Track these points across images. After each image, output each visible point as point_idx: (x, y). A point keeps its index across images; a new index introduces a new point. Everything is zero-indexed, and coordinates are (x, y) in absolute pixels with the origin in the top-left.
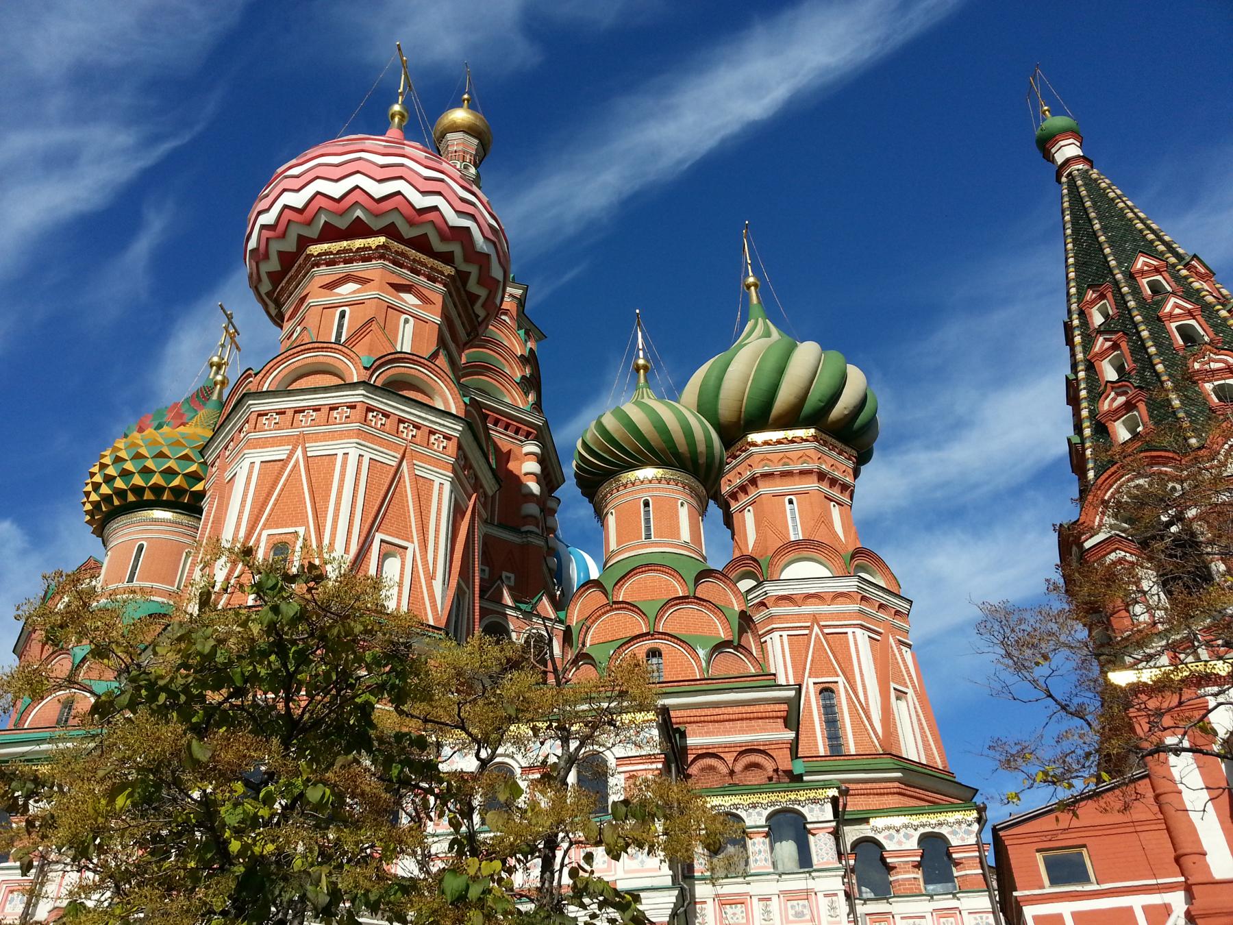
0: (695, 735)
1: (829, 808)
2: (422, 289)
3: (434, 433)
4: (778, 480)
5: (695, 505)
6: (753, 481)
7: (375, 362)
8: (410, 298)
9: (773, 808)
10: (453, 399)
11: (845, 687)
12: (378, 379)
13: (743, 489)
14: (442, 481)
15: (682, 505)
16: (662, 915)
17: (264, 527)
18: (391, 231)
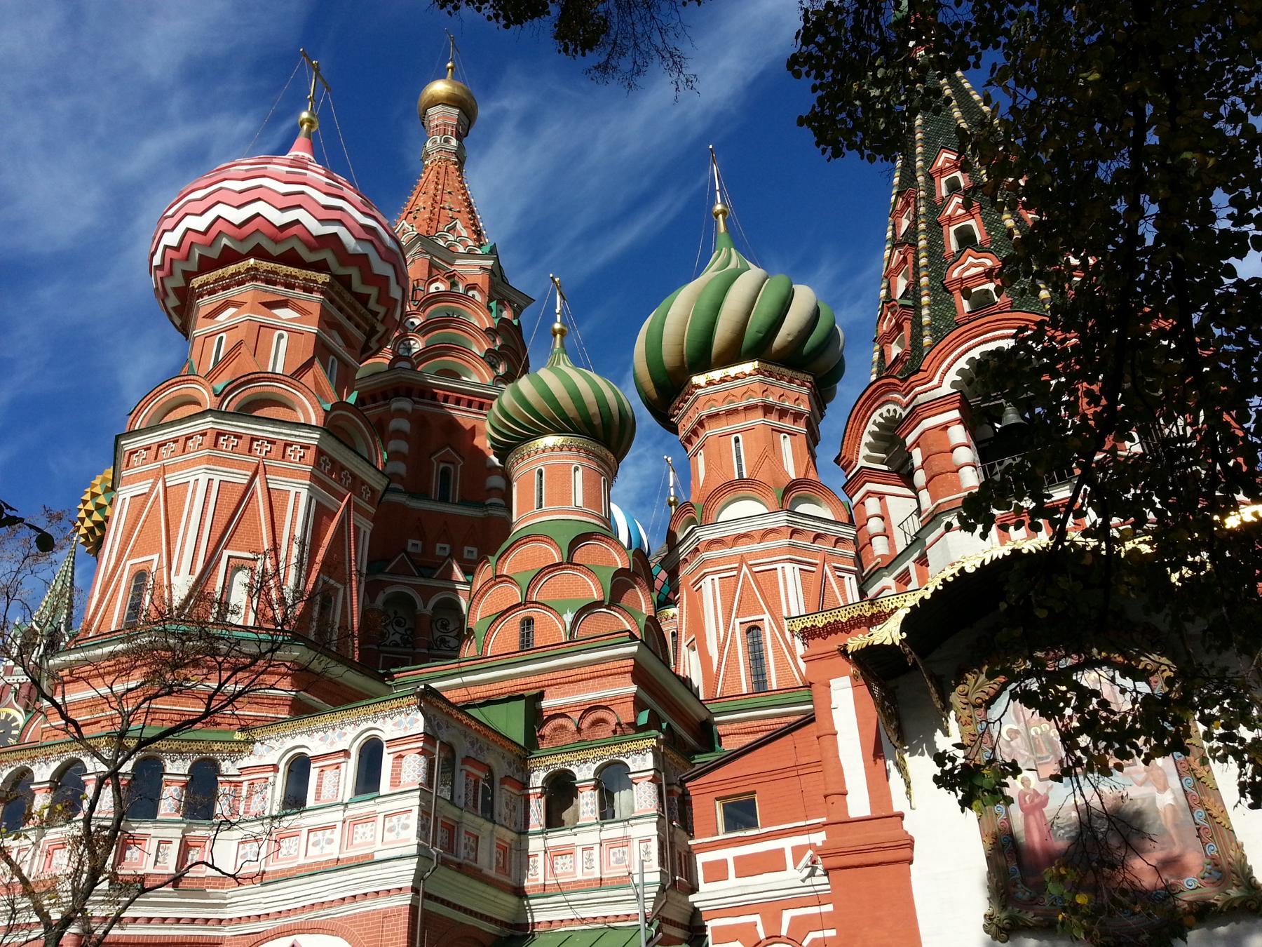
0: (552, 697)
1: (650, 757)
2: (298, 302)
3: (291, 446)
4: (724, 420)
5: (594, 466)
6: (701, 424)
8: (285, 313)
9: (601, 762)
10: (313, 408)
12: (230, 404)
13: (695, 432)
14: (298, 490)
15: (576, 469)
16: (407, 881)
17: (129, 557)
18: (259, 253)
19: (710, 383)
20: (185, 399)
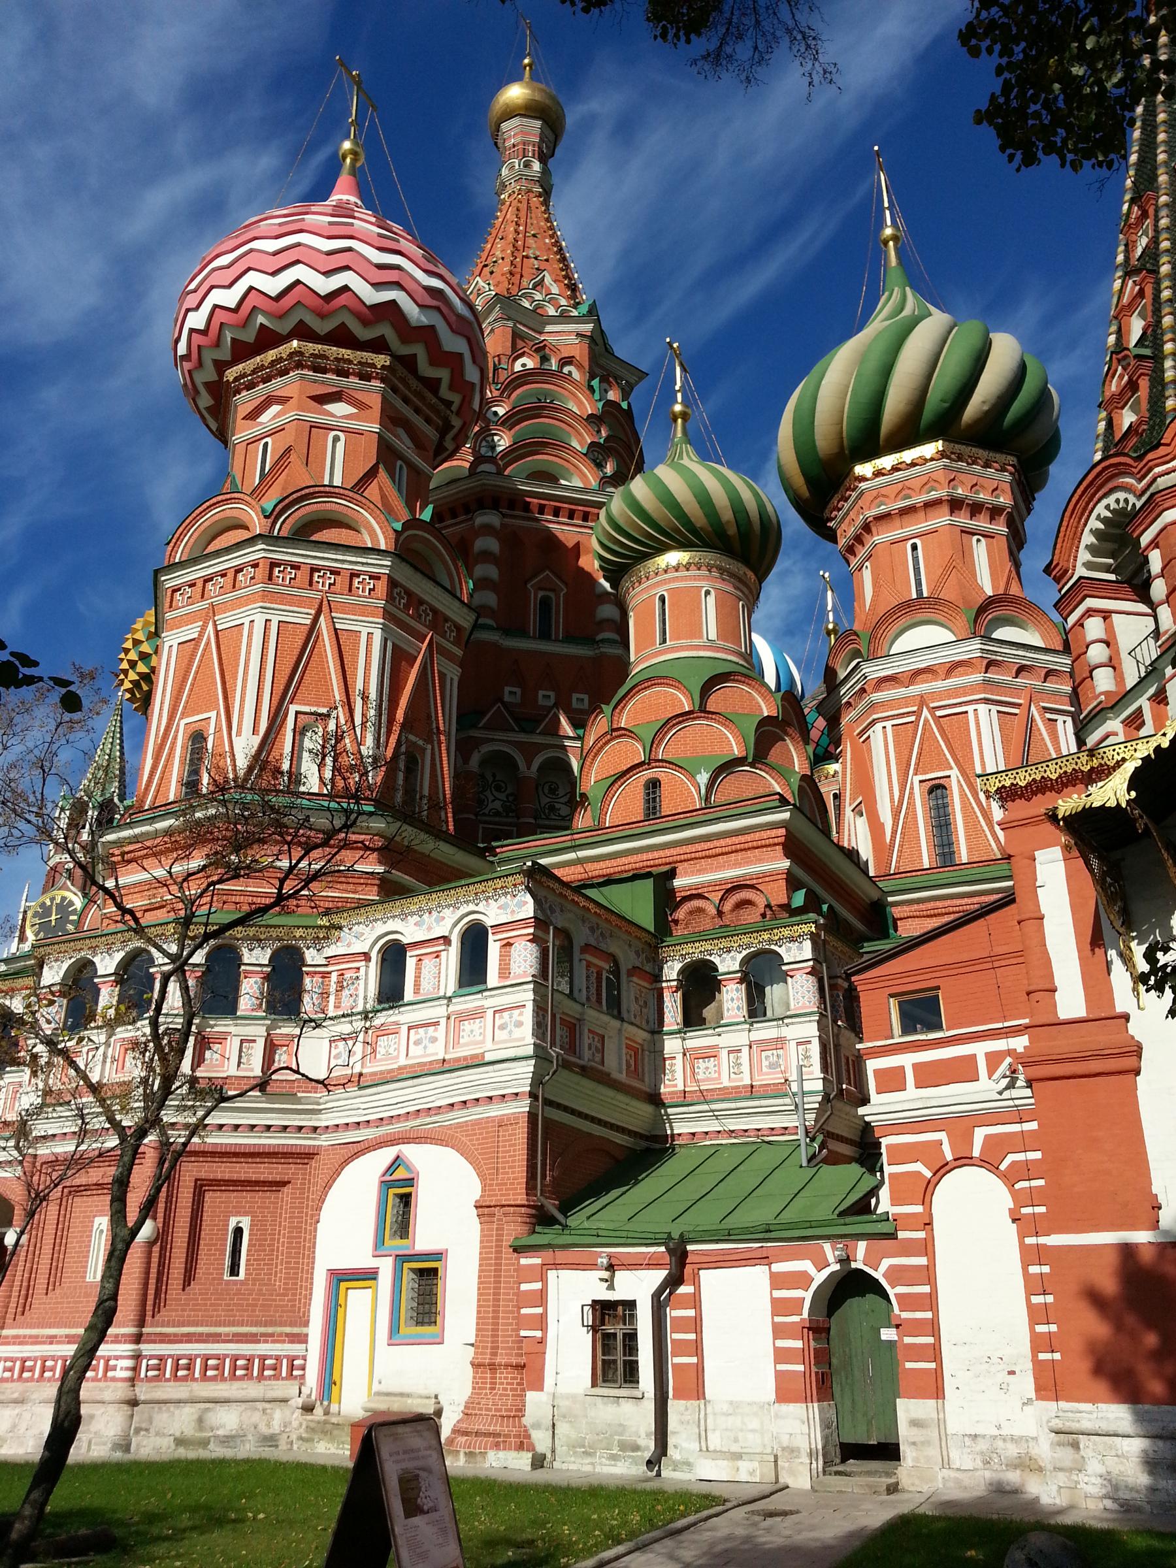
0: (686, 874)
1: (807, 945)
3: (358, 576)
4: (897, 522)
5: (730, 589)
6: (867, 528)
7: (276, 506)
8: (340, 409)
9: (748, 951)
10: (381, 528)
11: (959, 781)
12: (283, 527)
13: (859, 539)
14: (371, 630)
15: (707, 593)
16: (523, 1085)
18: (303, 332)
19: (878, 473)
20: (230, 523)
